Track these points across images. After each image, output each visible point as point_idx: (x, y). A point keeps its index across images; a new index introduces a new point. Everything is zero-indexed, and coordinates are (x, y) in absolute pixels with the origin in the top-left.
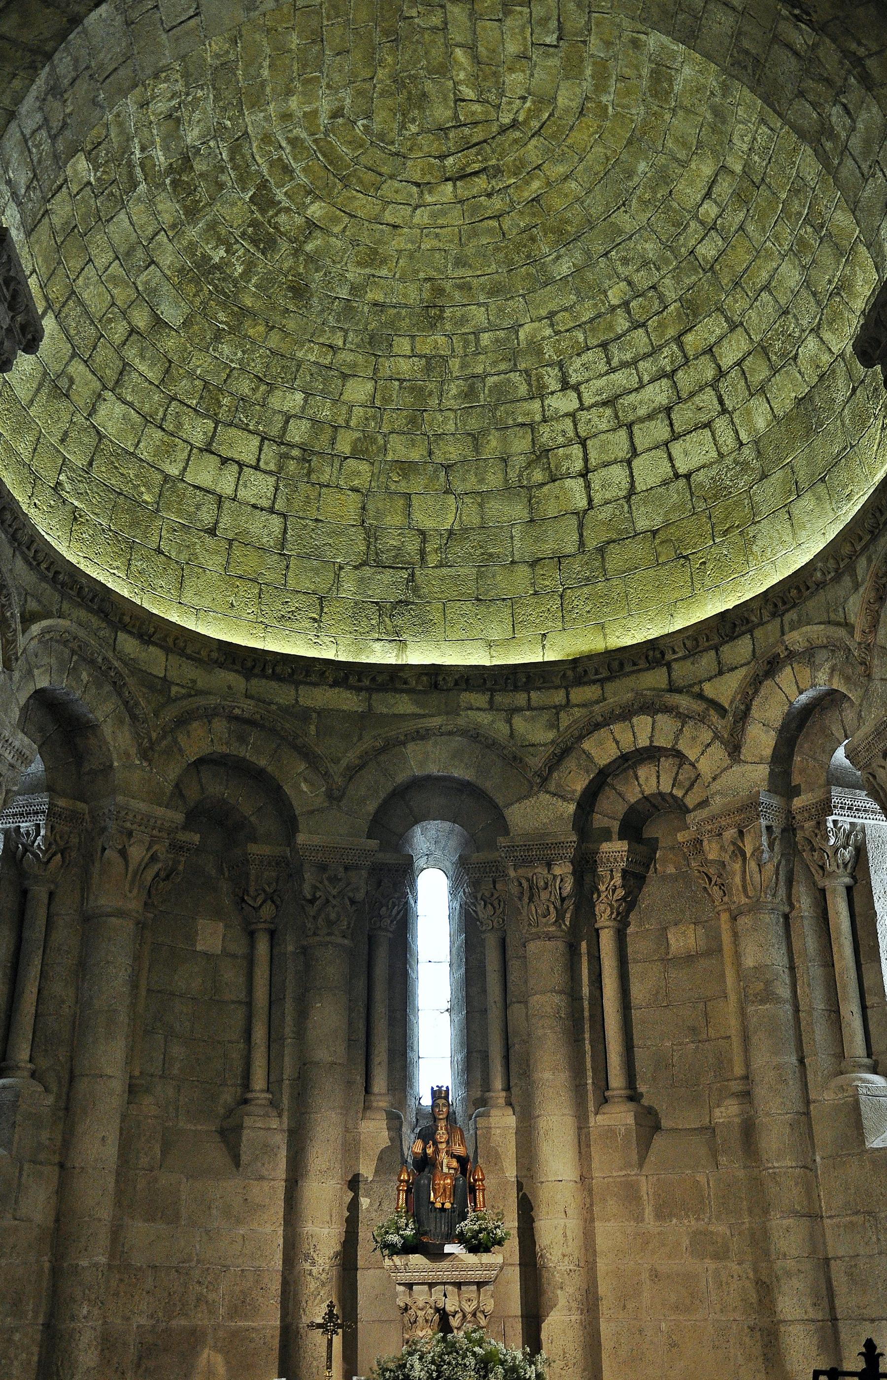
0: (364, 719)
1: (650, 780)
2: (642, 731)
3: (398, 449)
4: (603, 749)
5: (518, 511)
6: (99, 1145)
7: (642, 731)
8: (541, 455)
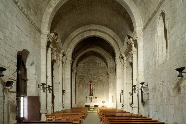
0: (88, 76)
1: (101, 79)
2: (100, 77)
3: (89, 62)
4: (98, 78)
5: (95, 65)
6: (77, 95)
7: (100, 77)
8: (96, 62)
